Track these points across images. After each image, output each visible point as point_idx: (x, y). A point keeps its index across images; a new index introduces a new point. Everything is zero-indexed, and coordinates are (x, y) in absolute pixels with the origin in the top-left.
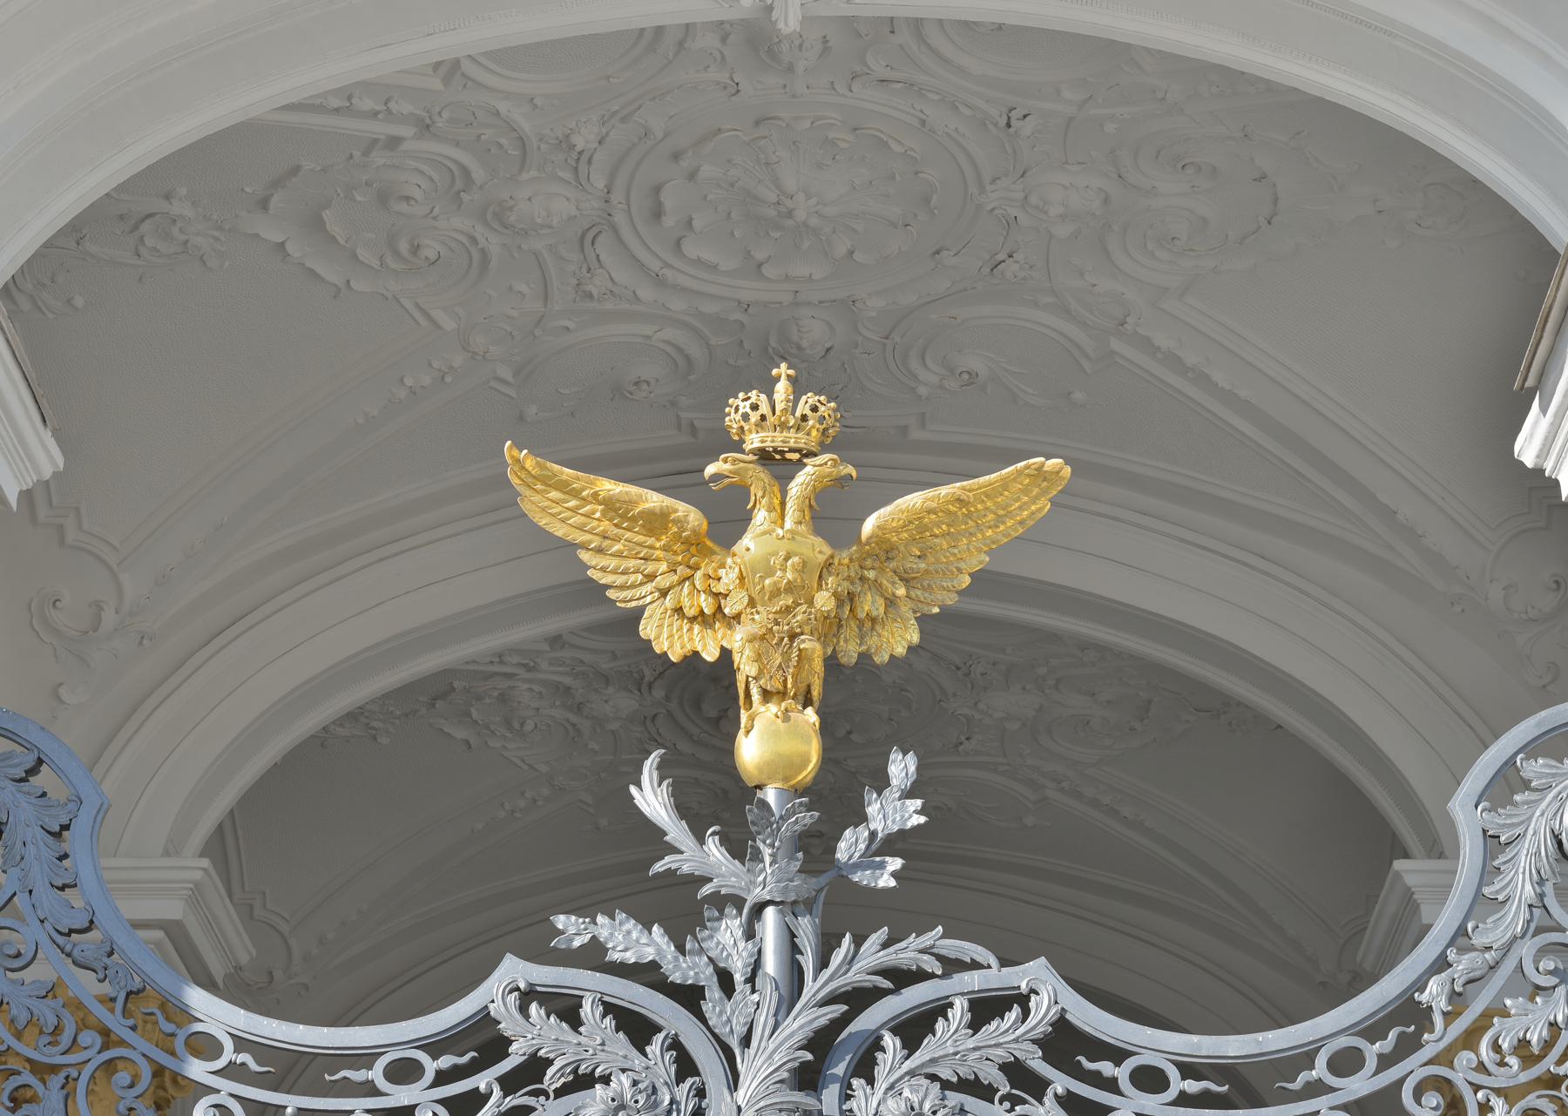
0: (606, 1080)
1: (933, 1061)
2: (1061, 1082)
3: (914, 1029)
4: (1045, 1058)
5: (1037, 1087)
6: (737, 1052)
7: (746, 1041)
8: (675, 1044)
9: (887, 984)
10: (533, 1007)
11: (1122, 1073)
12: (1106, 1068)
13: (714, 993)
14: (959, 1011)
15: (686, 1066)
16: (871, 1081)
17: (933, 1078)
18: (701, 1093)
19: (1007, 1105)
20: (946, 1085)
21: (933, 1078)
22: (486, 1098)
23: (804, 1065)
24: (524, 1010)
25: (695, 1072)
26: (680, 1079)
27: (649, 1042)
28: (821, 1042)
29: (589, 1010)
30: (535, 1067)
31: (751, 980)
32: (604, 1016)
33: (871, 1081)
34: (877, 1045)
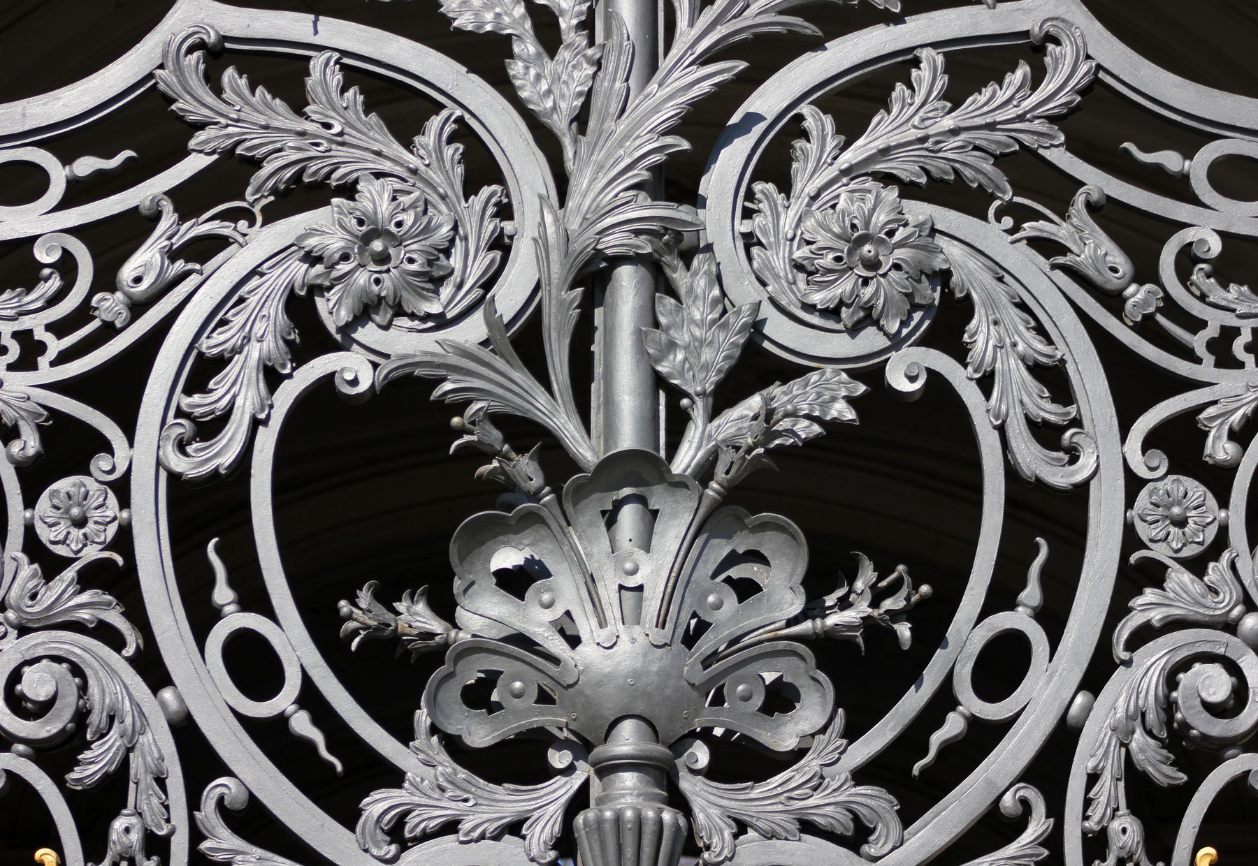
0: (349, 190)
1: (885, 152)
2: (1097, 182)
3: (855, 101)
4: (1072, 146)
5: (1059, 192)
6: (567, 142)
7: (581, 120)
8: (463, 133)
9: (810, 29)
10: (229, 74)
11: (1198, 167)
12: (1170, 160)
13: (527, 47)
14: (929, 74)
15: (481, 168)
16: (785, 187)
17: (887, 179)
18: (504, 211)
19: (1008, 222)
20: (909, 190)
21: (887, 179)
22: (156, 217)
23: (676, 158)
24: (213, 81)
25: (496, 176)
26: (470, 189)
27: (419, 129)
28: (706, 124)
29: (322, 76)
30: (233, 170)
31: (587, 25)
32: (344, 90)
33: (785, 187)
34: (793, 128)
